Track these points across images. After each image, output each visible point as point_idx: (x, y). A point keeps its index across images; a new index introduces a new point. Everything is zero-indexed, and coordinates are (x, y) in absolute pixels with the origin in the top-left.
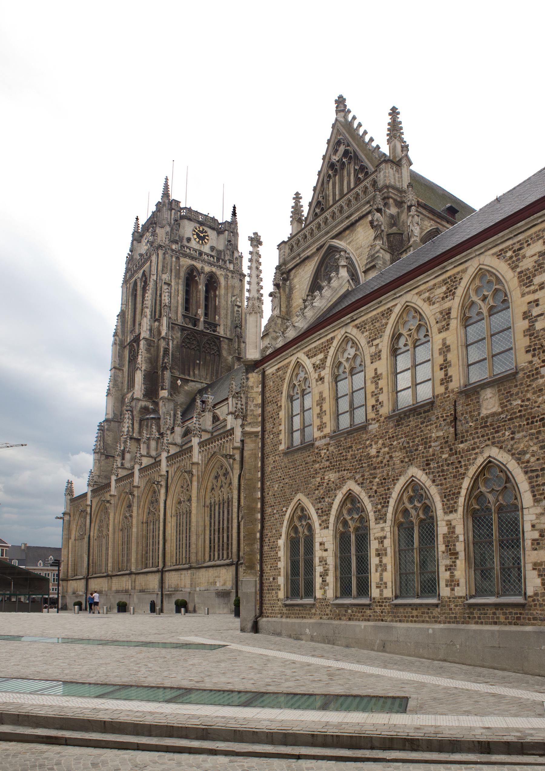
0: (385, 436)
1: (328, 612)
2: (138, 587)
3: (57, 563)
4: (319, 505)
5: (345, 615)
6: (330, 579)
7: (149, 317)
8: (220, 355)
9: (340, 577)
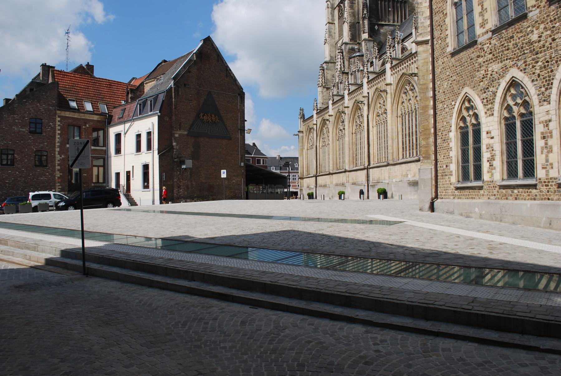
0: (546, 20)
1: (495, 193)
2: (351, 181)
3: (287, 164)
4: (484, 95)
5: (511, 195)
6: (497, 163)
9: (507, 162)
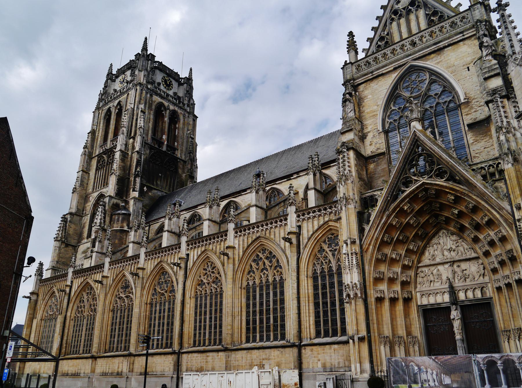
7: (125, 134)
8: (177, 172)
